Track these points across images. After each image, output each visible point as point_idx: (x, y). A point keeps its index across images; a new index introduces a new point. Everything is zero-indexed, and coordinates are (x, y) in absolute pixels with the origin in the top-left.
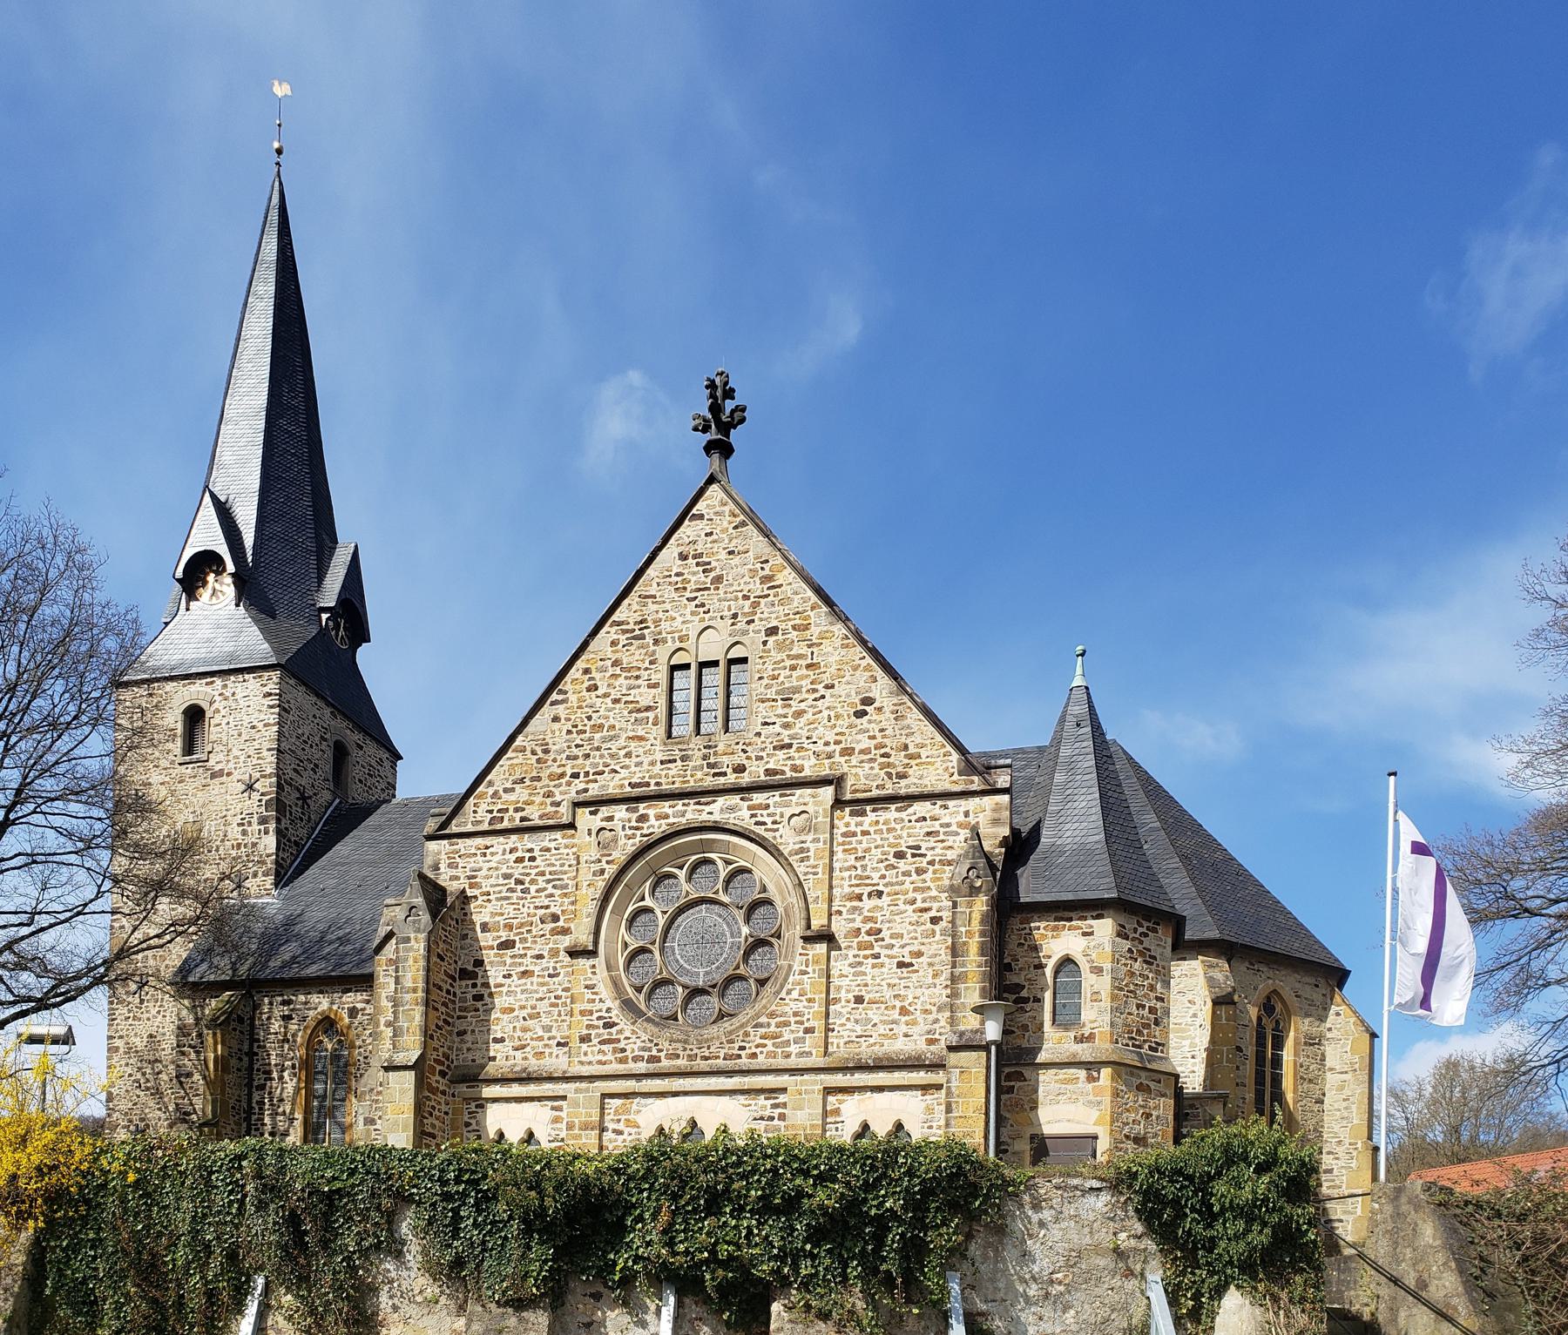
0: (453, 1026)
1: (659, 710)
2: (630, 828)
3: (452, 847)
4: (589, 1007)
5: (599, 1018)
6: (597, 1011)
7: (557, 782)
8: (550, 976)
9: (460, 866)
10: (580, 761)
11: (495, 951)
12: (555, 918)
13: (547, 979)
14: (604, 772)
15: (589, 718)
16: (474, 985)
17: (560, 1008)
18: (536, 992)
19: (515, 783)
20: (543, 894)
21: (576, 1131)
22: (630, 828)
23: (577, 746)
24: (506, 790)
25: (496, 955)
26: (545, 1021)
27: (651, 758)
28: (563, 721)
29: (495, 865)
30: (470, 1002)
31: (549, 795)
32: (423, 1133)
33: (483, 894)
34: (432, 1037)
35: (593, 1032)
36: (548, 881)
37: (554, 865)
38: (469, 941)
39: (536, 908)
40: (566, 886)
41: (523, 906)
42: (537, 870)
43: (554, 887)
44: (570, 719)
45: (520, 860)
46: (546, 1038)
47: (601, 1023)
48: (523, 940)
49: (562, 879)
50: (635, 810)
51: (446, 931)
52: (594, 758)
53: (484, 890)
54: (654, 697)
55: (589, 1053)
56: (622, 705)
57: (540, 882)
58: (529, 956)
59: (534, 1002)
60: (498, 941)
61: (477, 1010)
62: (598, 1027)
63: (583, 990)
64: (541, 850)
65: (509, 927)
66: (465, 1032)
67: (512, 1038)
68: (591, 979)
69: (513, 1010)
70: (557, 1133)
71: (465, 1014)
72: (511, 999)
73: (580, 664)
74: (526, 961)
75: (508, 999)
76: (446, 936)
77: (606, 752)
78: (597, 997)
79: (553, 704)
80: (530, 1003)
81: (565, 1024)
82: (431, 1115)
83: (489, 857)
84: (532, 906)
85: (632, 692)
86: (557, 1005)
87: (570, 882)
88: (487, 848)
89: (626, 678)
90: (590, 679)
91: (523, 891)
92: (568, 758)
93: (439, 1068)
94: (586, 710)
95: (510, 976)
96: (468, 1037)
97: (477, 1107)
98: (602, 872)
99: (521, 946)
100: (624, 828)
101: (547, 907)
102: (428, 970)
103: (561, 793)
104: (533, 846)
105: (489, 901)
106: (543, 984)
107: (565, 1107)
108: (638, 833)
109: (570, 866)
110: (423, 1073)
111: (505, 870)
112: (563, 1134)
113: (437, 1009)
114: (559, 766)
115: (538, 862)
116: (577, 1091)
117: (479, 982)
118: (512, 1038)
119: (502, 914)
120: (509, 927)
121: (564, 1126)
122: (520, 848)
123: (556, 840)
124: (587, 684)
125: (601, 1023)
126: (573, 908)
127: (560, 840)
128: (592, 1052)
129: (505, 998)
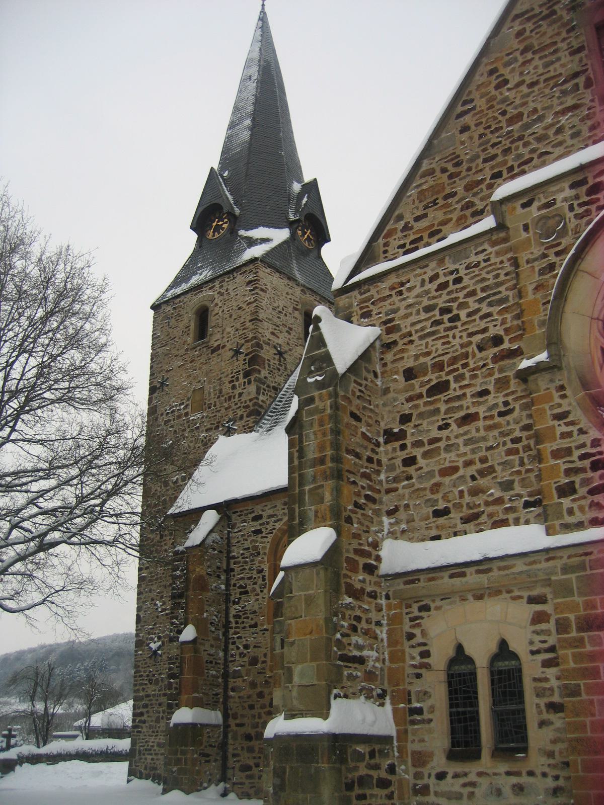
0: (381, 503)
1: (590, 71)
2: (580, 205)
3: (364, 296)
4: (565, 443)
5: (583, 457)
6: (578, 447)
7: (475, 190)
8: (501, 414)
9: (374, 313)
10: (500, 159)
11: (426, 399)
12: (497, 340)
13: (497, 420)
14: (532, 159)
15: (504, 113)
16: (403, 447)
17: (521, 454)
18: (484, 439)
19: (426, 207)
20: (477, 317)
21: (574, 634)
22: (580, 205)
23: (493, 146)
24: (417, 219)
25: (426, 404)
26: (504, 475)
27: (589, 123)
28: (473, 128)
29: (410, 301)
30: (400, 469)
31: (469, 205)
32: (345, 658)
33: (404, 336)
34: (349, 520)
35: (577, 479)
36: (481, 301)
37: (484, 280)
38: (391, 395)
39: (471, 335)
40: (506, 299)
41: (454, 337)
42: (465, 292)
43: (490, 304)
44: (481, 123)
45: (443, 286)
46: (507, 498)
47: (587, 463)
48: (458, 378)
49: (500, 292)
50: (584, 182)
51: (361, 385)
52: (517, 148)
53: (404, 331)
54: (581, 60)
55: (576, 510)
56: (542, 85)
57: (471, 304)
58: (468, 395)
59: (483, 453)
60: (428, 387)
61: (409, 478)
62: (583, 470)
63: (551, 423)
64: (467, 268)
65: (439, 366)
66: (396, 509)
67: (458, 506)
68: (560, 405)
69: (455, 469)
70: (542, 638)
71: (395, 485)
72: (452, 456)
73: (484, 69)
74: (469, 401)
75: (447, 456)
76: (360, 391)
77: (531, 139)
78: (575, 429)
79: (460, 116)
80: (477, 457)
81: (532, 476)
82: (354, 629)
83: (405, 295)
84: (464, 334)
85: (551, 68)
86: (516, 452)
87: (510, 293)
88: (402, 284)
89: (541, 58)
90: (498, 77)
91: (450, 320)
92: (485, 161)
93: (362, 561)
94: (499, 106)
95: (446, 426)
96: (402, 515)
97: (421, 609)
98: (552, 267)
99: (457, 386)
100: (571, 208)
101: (485, 330)
102: (336, 432)
103: (482, 199)
104: (457, 266)
105: (411, 342)
106: (489, 428)
107: (549, 596)
108: (593, 207)
109: (506, 274)
110: (337, 575)
111: (426, 302)
112: (552, 640)
113: (354, 483)
114: (477, 172)
115: (466, 281)
116: (565, 570)
117: (408, 442)
118: (458, 506)
119: (428, 354)
120: (439, 366)
121: (551, 626)
122: (441, 273)
123: (485, 250)
124: (494, 83)
125: (587, 463)
126: (519, 322)
127: (490, 250)
128: (581, 509)
129: (443, 455)
